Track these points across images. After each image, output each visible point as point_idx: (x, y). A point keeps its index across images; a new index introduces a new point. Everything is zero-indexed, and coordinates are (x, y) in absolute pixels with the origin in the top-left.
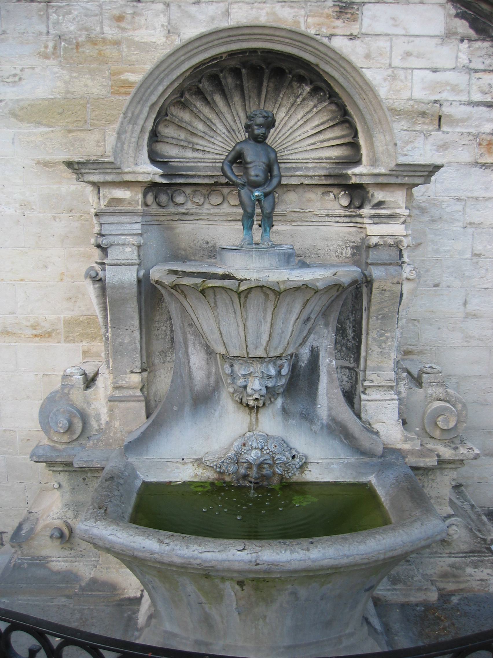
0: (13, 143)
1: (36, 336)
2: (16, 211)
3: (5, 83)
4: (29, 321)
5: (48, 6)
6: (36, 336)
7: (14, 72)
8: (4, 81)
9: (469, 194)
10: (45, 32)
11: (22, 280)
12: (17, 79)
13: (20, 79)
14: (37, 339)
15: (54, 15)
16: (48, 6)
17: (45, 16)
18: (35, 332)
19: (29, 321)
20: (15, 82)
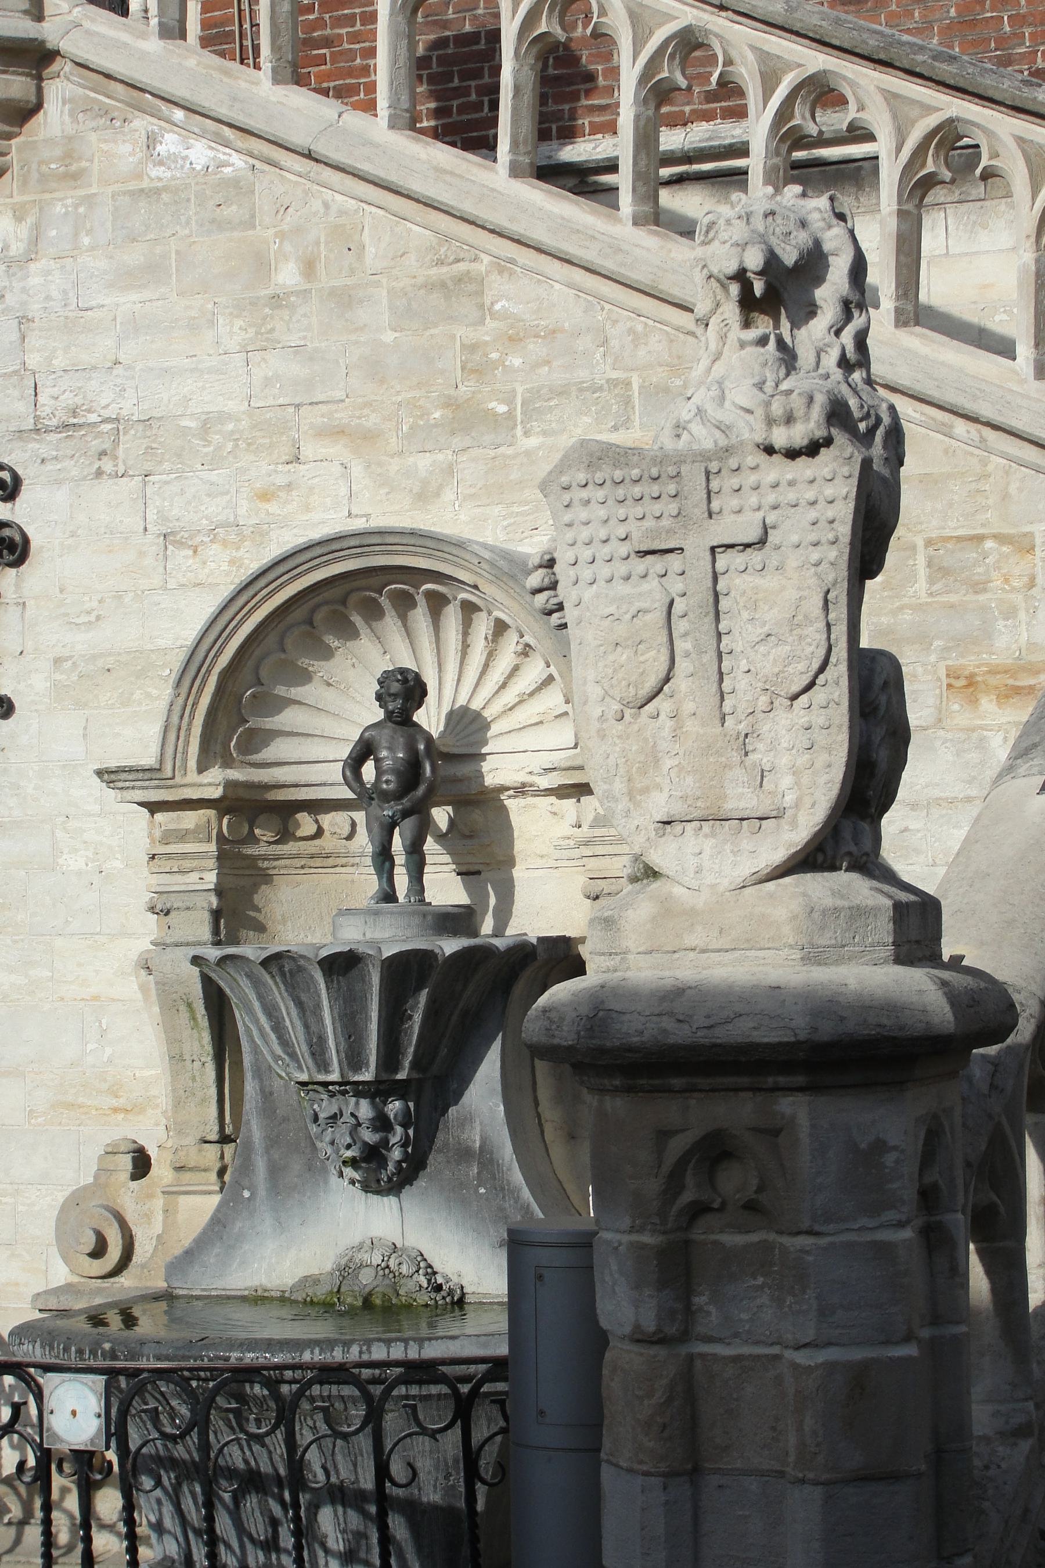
0: (85, 736)
1: (115, 1110)
2: (87, 865)
3: (73, 626)
4: (105, 1080)
5: (145, 483)
6: (115, 1110)
7: (87, 606)
8: (71, 623)
9: (937, 793)
10: (141, 530)
11: (96, 998)
12: (93, 619)
13: (98, 618)
14: (120, 1116)
15: (156, 497)
16: (145, 483)
17: (141, 502)
18: (115, 1103)
19: (105, 1080)
20: (90, 622)
